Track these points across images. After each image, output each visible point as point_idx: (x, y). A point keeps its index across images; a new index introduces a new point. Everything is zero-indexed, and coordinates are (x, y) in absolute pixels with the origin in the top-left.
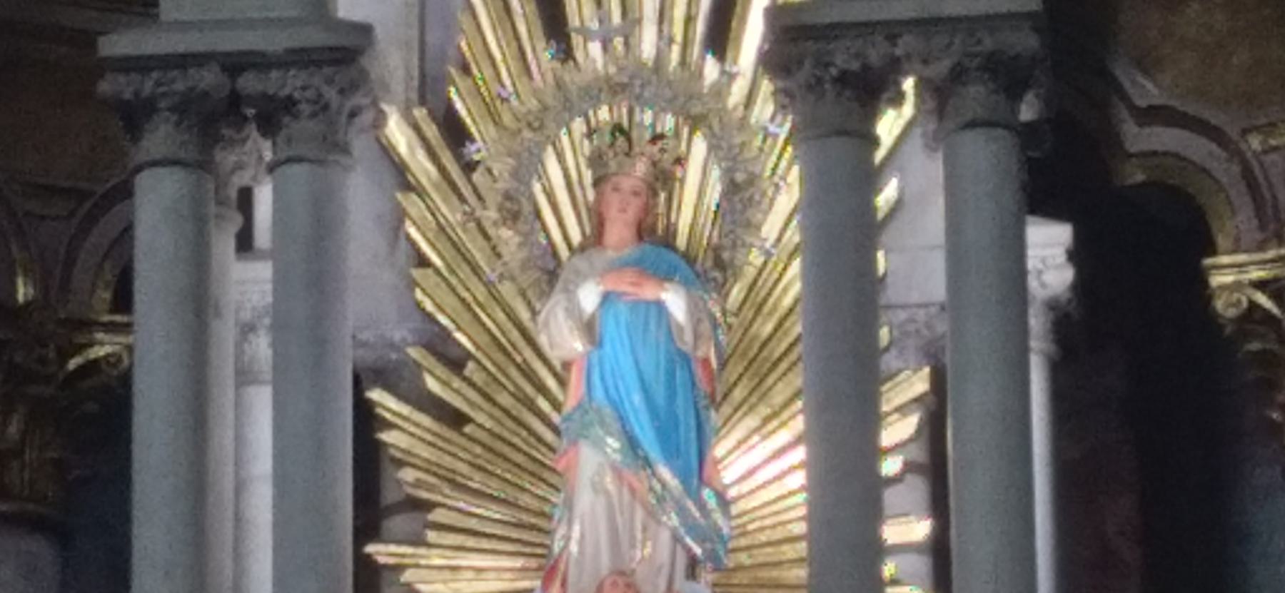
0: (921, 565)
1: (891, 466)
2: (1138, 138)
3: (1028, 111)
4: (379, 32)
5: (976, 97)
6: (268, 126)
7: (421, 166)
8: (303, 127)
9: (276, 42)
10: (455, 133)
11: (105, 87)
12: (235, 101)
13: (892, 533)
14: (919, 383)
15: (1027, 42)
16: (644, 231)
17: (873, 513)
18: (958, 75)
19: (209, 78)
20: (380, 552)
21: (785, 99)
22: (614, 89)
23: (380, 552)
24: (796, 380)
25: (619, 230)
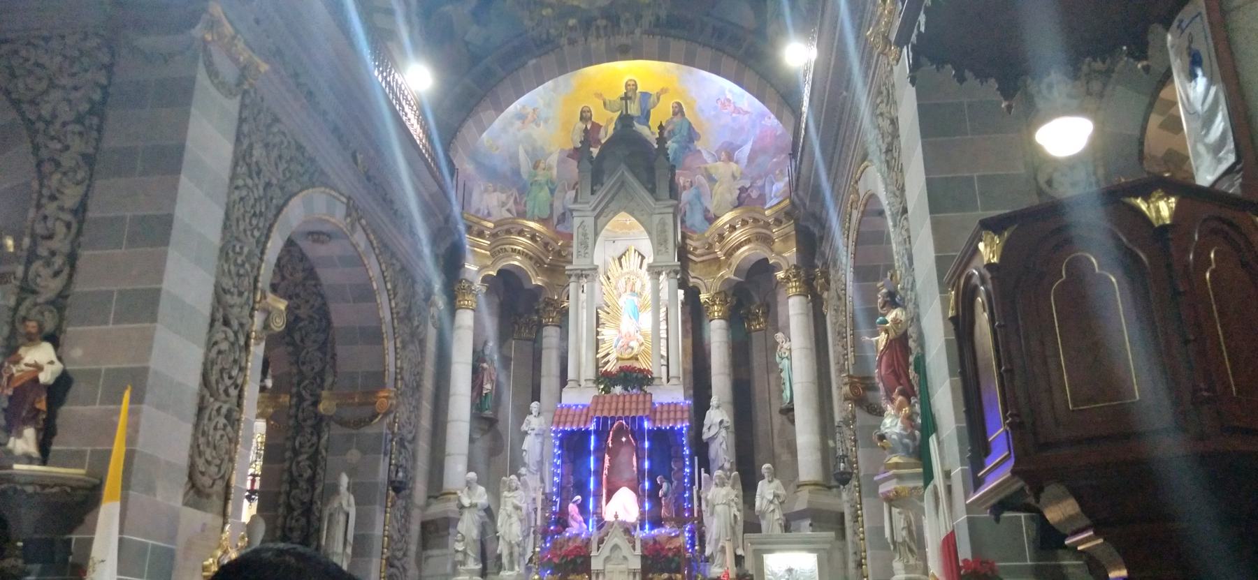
0: (665, 331)
1: (661, 319)
2: (691, 280)
3: (678, 277)
4: (600, 267)
5: (672, 275)
6: (586, 277)
7: (604, 283)
8: (590, 278)
9: (586, 267)
10: (609, 279)
11: (566, 272)
12: (582, 275)
13: (661, 328)
14: (665, 309)
15: (679, 268)
16: (631, 290)
17: (659, 325)
18: (670, 272)
19: (579, 272)
20: (599, 329)
21: (649, 274)
22: (628, 273)
23: (599, 329)
24: (650, 309)
25: (628, 292)
